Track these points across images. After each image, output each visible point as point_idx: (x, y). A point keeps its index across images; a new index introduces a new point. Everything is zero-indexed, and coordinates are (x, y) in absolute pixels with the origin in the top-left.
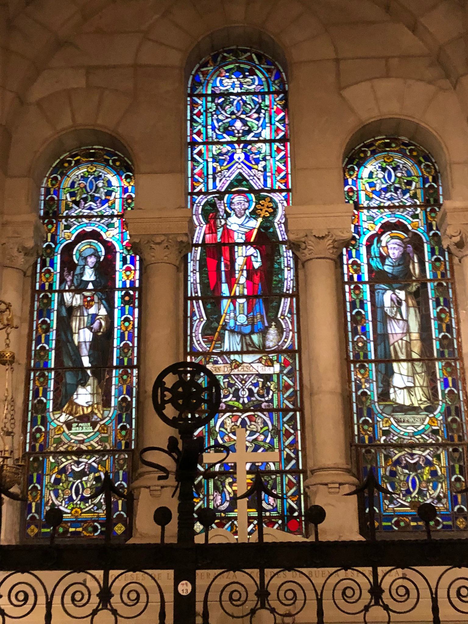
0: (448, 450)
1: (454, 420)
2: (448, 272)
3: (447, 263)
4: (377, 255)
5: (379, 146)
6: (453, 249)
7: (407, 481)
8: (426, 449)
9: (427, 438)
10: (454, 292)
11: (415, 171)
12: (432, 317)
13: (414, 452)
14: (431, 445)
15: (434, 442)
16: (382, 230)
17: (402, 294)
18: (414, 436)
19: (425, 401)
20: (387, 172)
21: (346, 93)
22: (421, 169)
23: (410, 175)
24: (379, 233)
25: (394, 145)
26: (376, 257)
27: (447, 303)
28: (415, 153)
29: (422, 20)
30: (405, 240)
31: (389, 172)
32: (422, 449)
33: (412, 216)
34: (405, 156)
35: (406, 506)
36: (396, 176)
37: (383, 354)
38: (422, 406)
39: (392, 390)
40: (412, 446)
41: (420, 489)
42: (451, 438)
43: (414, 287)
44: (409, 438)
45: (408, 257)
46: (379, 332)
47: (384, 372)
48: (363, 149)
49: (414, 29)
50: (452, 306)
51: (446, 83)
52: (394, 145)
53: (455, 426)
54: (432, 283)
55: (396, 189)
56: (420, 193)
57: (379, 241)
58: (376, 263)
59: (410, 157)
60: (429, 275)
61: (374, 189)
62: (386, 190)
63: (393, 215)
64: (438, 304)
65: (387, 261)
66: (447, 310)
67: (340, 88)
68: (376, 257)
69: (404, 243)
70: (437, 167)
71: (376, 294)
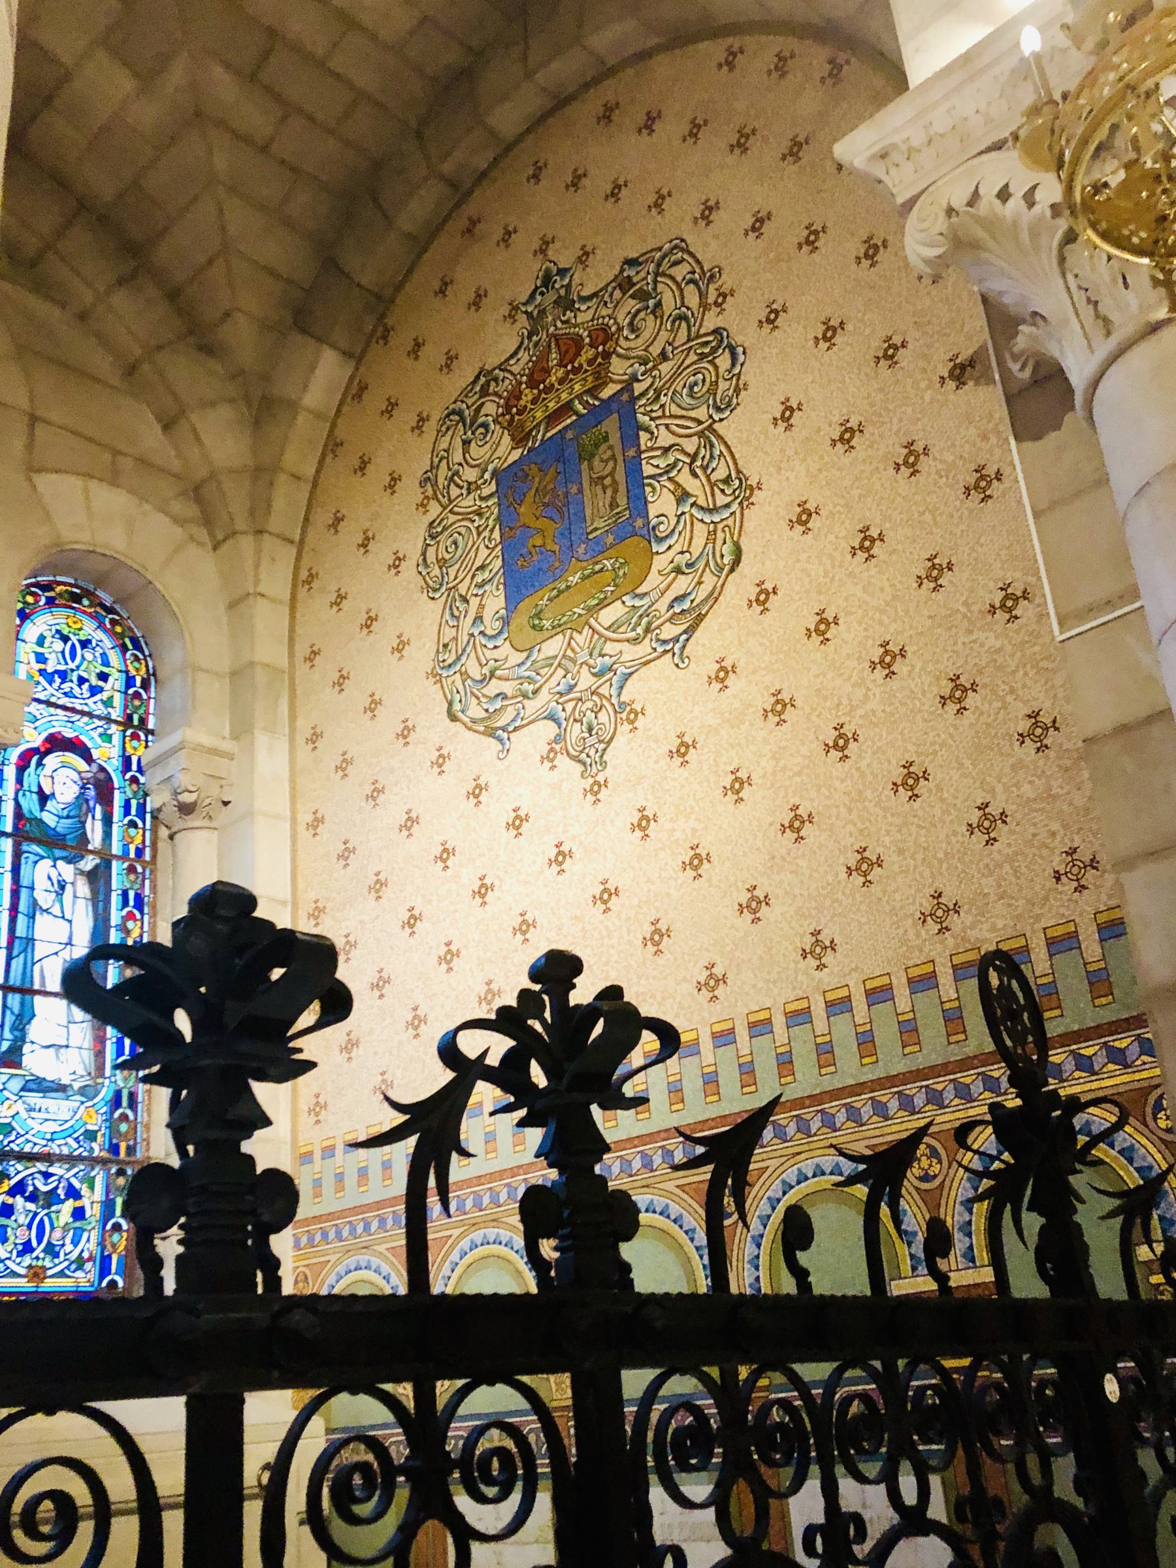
0: (109, 1170)
1: (124, 1117)
2: (148, 851)
3: (148, 834)
4: (35, 789)
5: (60, 595)
6: (170, 813)
7: (29, 1226)
8: (73, 1166)
9: (77, 1146)
10: (154, 888)
11: (114, 657)
12: (113, 923)
13: (51, 1170)
14: (80, 1159)
15: (85, 1154)
16: (48, 746)
17: (67, 871)
18: (52, 1140)
19: (82, 1076)
20: (69, 643)
21: (44, 482)
22: (125, 660)
23: (106, 663)
24: (42, 749)
25: (86, 602)
26: (30, 791)
27: (139, 904)
28: (118, 629)
29: (194, 418)
30: (83, 775)
31: (73, 645)
32: (67, 1166)
33: (101, 735)
34: (101, 626)
35: (20, 1276)
36: (83, 658)
37: (19, 977)
38: (76, 1086)
39: (26, 1048)
40: (48, 1158)
41: (49, 1243)
42: (114, 1149)
43: (89, 863)
44: (44, 1142)
45: (85, 807)
46: (18, 934)
47: (16, 1011)
48: (33, 589)
49: (168, 426)
50: (146, 910)
51: (203, 534)
52: (86, 602)
53: (124, 1127)
54: (120, 862)
55: (82, 681)
56: (118, 699)
57: (40, 764)
58: (30, 804)
59: (111, 633)
60: (116, 849)
61: (42, 666)
62: (63, 675)
63: (70, 725)
64: (125, 903)
65: (49, 803)
66: (138, 916)
67: (32, 468)
68: (30, 791)
69: (82, 779)
70: (150, 664)
71: (23, 861)
